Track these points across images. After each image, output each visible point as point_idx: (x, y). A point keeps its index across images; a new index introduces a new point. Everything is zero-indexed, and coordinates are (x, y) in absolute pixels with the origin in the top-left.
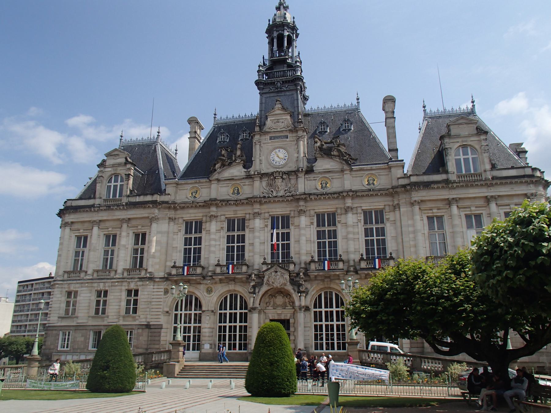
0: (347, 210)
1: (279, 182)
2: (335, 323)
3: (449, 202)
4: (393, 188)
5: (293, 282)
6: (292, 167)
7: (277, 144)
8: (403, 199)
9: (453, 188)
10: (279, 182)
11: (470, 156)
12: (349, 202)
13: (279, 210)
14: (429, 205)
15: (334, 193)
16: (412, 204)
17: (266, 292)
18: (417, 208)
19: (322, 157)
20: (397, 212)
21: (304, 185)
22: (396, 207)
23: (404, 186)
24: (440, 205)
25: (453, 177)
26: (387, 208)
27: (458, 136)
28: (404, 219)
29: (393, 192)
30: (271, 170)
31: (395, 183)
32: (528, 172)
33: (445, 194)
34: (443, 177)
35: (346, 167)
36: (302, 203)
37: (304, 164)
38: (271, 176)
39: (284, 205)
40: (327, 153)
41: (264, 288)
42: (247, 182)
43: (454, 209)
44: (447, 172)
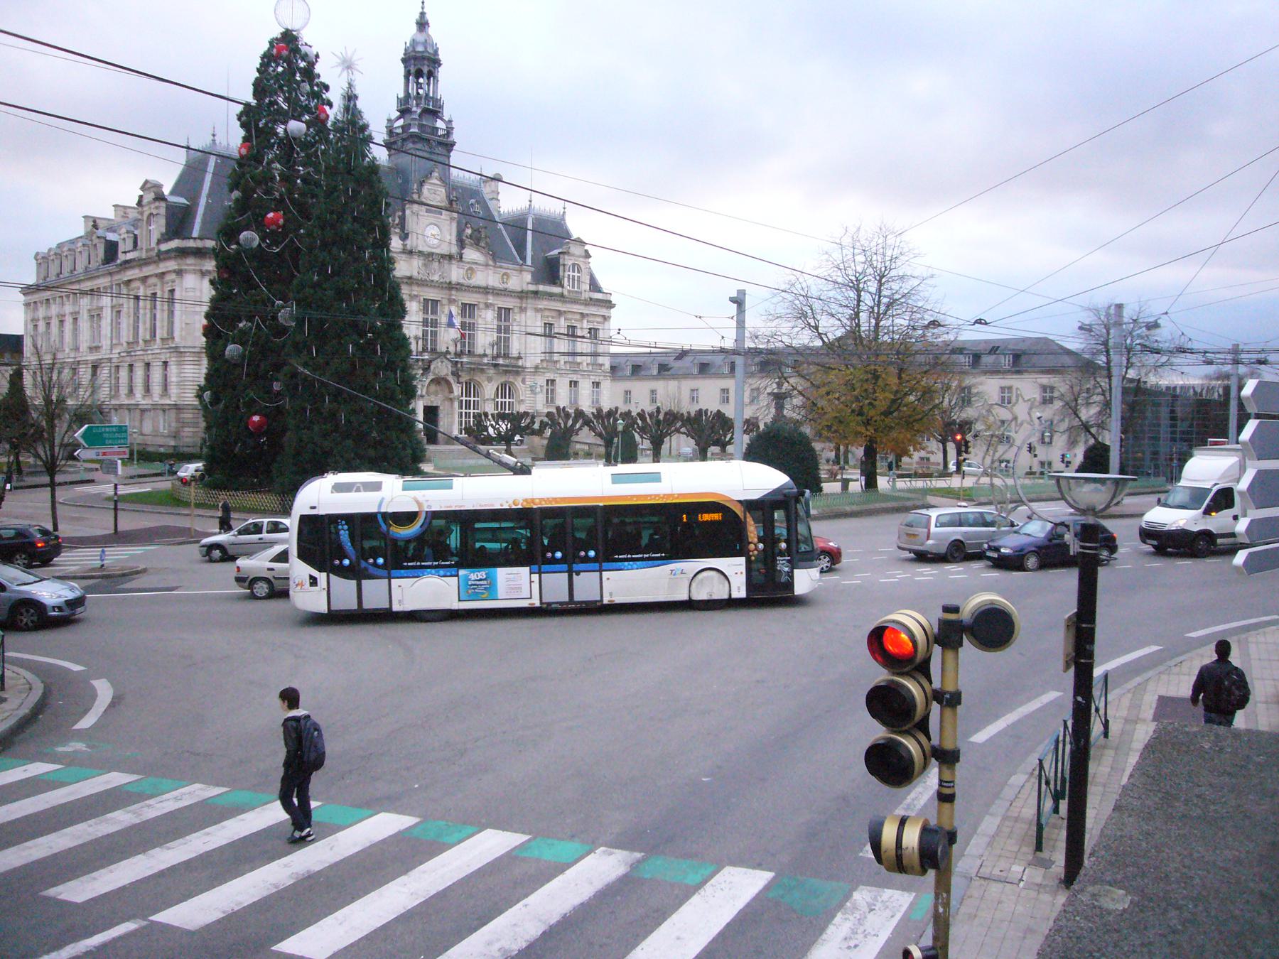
0: (487, 306)
1: (436, 265)
5: (453, 373)
6: (444, 250)
7: (433, 220)
8: (530, 303)
9: (565, 302)
10: (436, 265)
12: (491, 299)
13: (432, 294)
14: (547, 313)
16: (537, 310)
17: (432, 380)
18: (539, 316)
21: (455, 273)
23: (536, 293)
25: (566, 293)
26: (516, 310)
29: (522, 295)
30: (426, 249)
31: (525, 288)
32: (608, 298)
34: (556, 290)
35: (491, 263)
36: (453, 292)
37: (454, 250)
38: (428, 257)
39: (436, 290)
40: (476, 241)
41: (431, 377)
42: (404, 256)
43: (562, 319)
44: (562, 286)
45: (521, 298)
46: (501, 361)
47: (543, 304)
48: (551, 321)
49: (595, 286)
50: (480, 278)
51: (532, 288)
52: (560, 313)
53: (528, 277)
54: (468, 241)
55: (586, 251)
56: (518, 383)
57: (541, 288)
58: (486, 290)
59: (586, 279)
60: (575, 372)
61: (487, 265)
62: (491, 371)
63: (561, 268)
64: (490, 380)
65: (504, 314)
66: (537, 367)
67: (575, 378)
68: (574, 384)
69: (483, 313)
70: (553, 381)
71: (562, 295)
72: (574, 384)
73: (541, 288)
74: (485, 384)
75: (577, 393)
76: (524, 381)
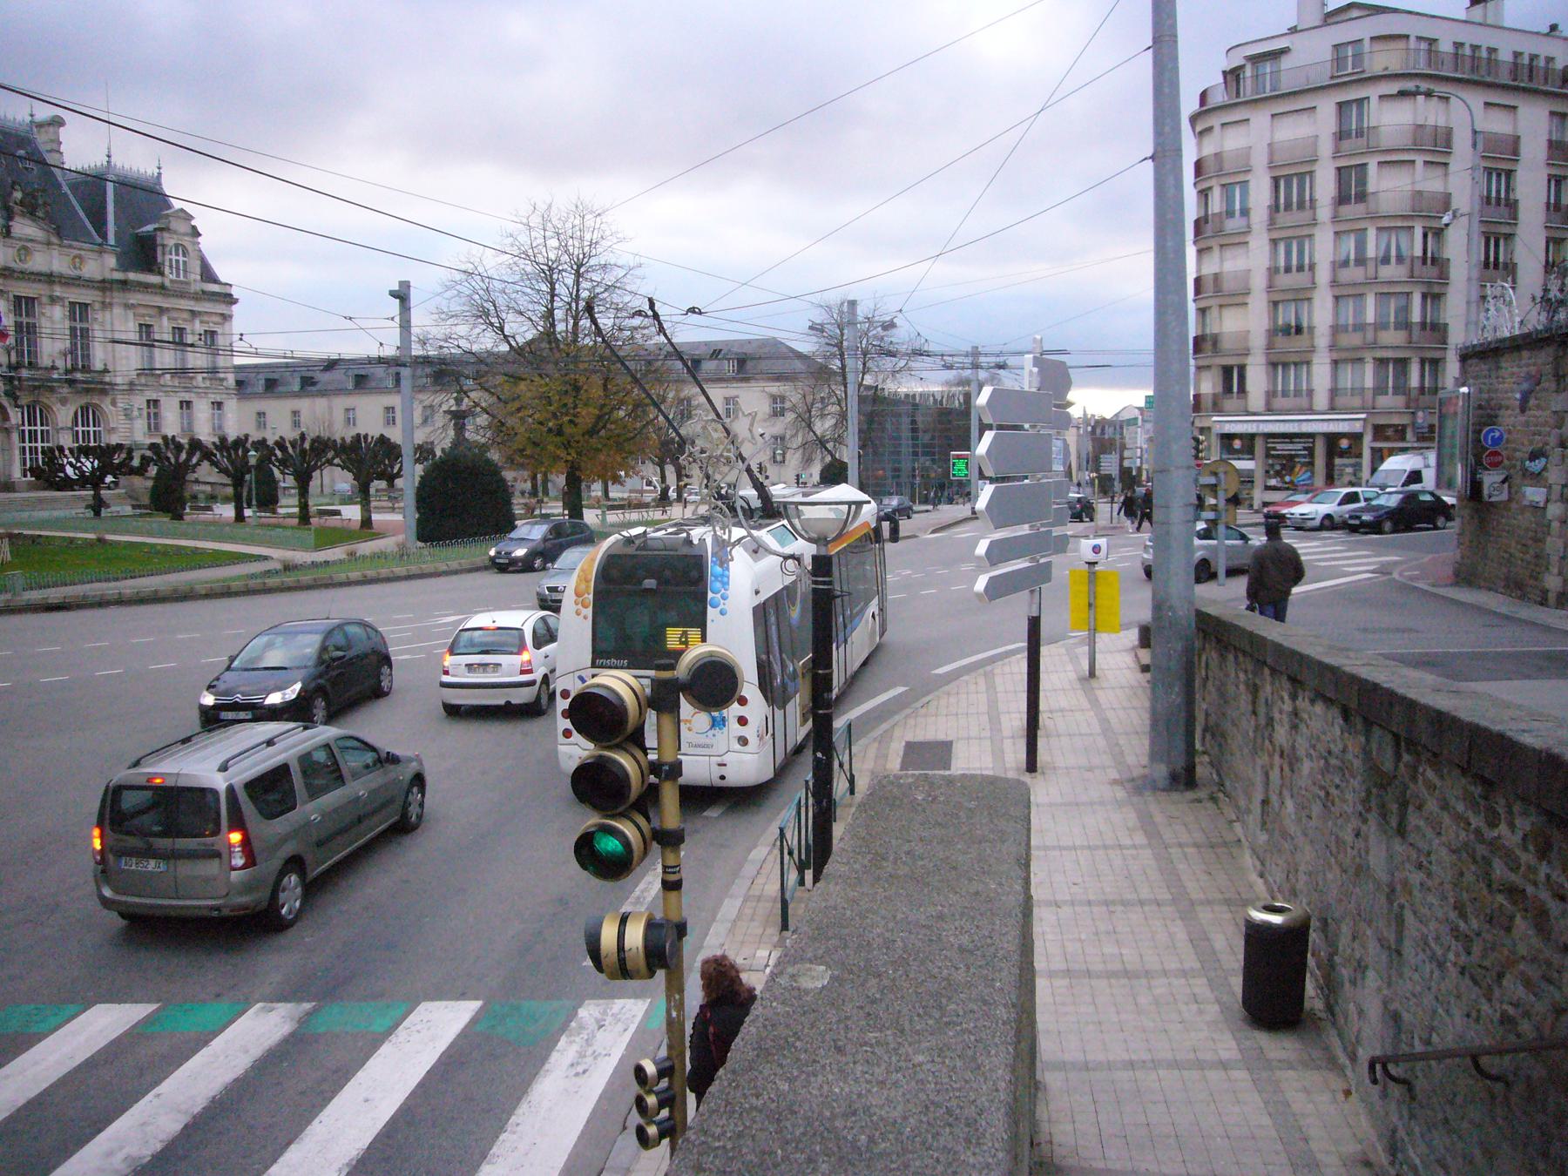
0: (53, 300)
2: (40, 445)
3: (162, 311)
4: (103, 281)
8: (118, 297)
11: (181, 258)
12: (58, 291)
14: (142, 311)
15: (39, 274)
16: (127, 306)
18: (130, 314)
19: (23, 215)
20: (108, 315)
22: (106, 306)
23: (124, 283)
24: (150, 311)
25: (167, 283)
27: (175, 232)
28: (116, 322)
29: (105, 285)
31: (108, 276)
33: (158, 301)
34: (154, 279)
35: (54, 240)
43: (165, 319)
44: (162, 274)
45: (103, 290)
46: (79, 376)
47: (135, 298)
48: (148, 321)
49: (208, 274)
50: (40, 261)
51: (119, 276)
52: (162, 311)
53: (111, 261)
54: (17, 209)
55: (194, 228)
56: (106, 405)
57: (132, 276)
58: (50, 278)
59: (195, 267)
60: (187, 389)
61: (49, 244)
62: (65, 390)
63: (159, 250)
64: (64, 401)
65: (79, 311)
66: (131, 384)
67: (187, 397)
68: (186, 405)
69: (47, 310)
70: (156, 402)
71: (162, 287)
72: (186, 405)
73: (132, 276)
74: (57, 407)
75: (190, 418)
76: (114, 403)
